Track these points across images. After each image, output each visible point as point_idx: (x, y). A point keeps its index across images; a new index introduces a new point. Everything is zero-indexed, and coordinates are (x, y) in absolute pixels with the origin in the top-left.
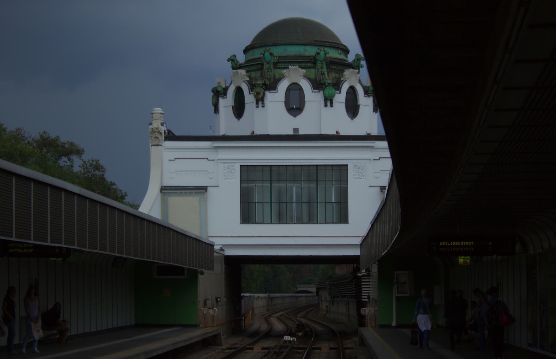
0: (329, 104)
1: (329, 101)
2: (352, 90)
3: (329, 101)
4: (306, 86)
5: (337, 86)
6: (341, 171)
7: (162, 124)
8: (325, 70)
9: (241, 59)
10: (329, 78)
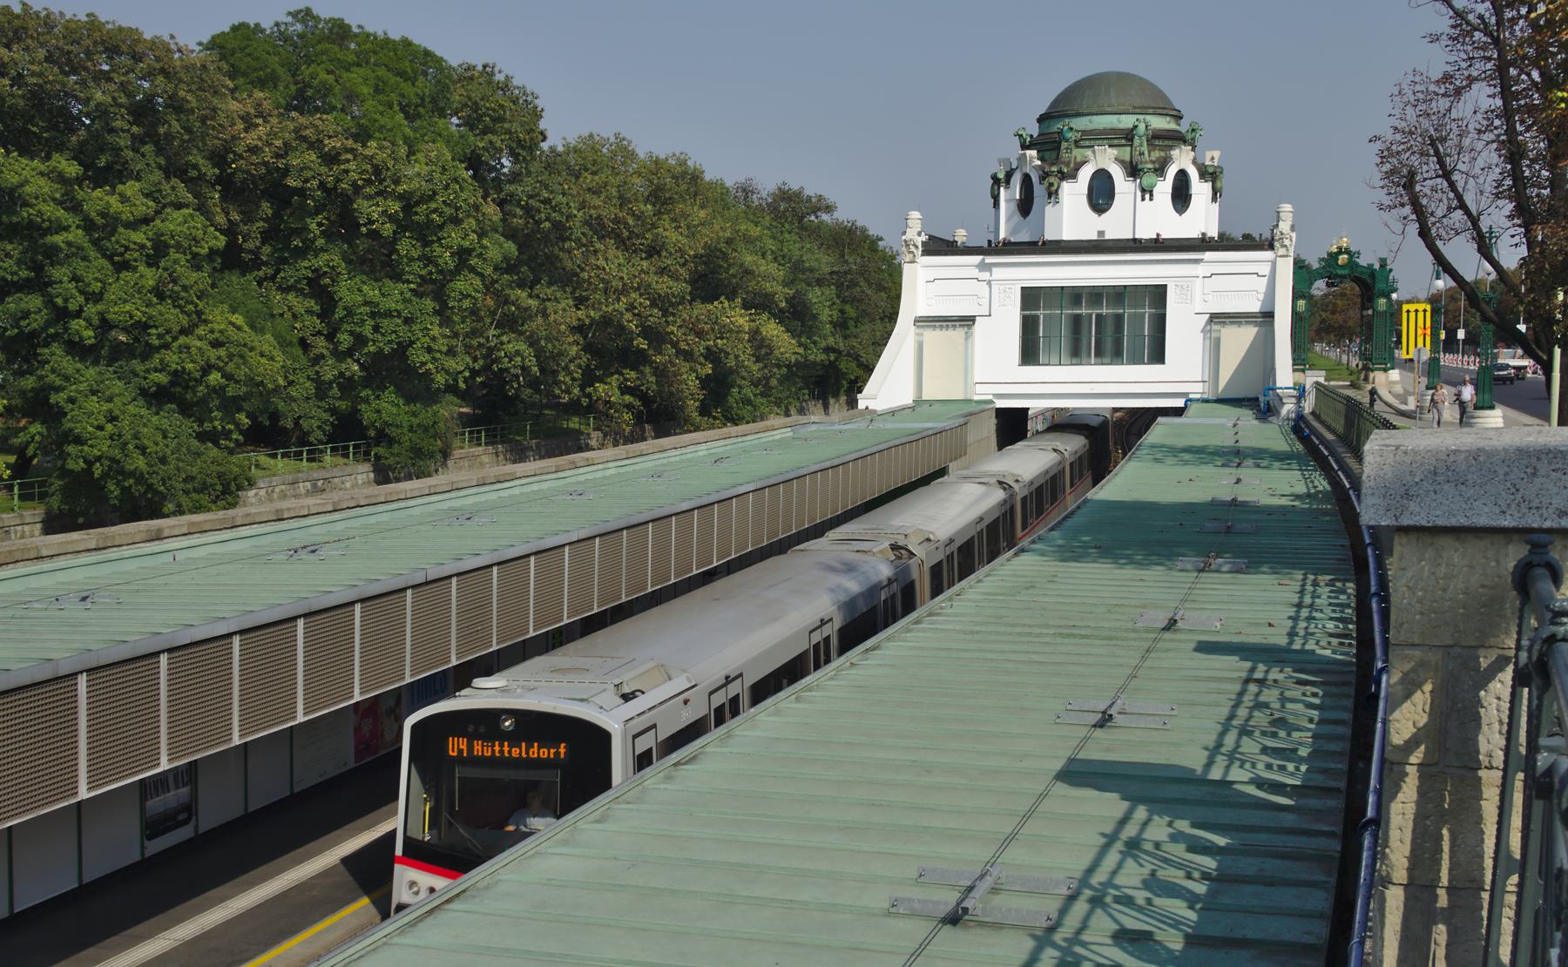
2: (1182, 177)
3: (1147, 192)
4: (1117, 173)
5: (1160, 171)
6: (1158, 294)
7: (919, 234)
8: (1145, 149)
9: (1034, 130)
10: (1149, 157)
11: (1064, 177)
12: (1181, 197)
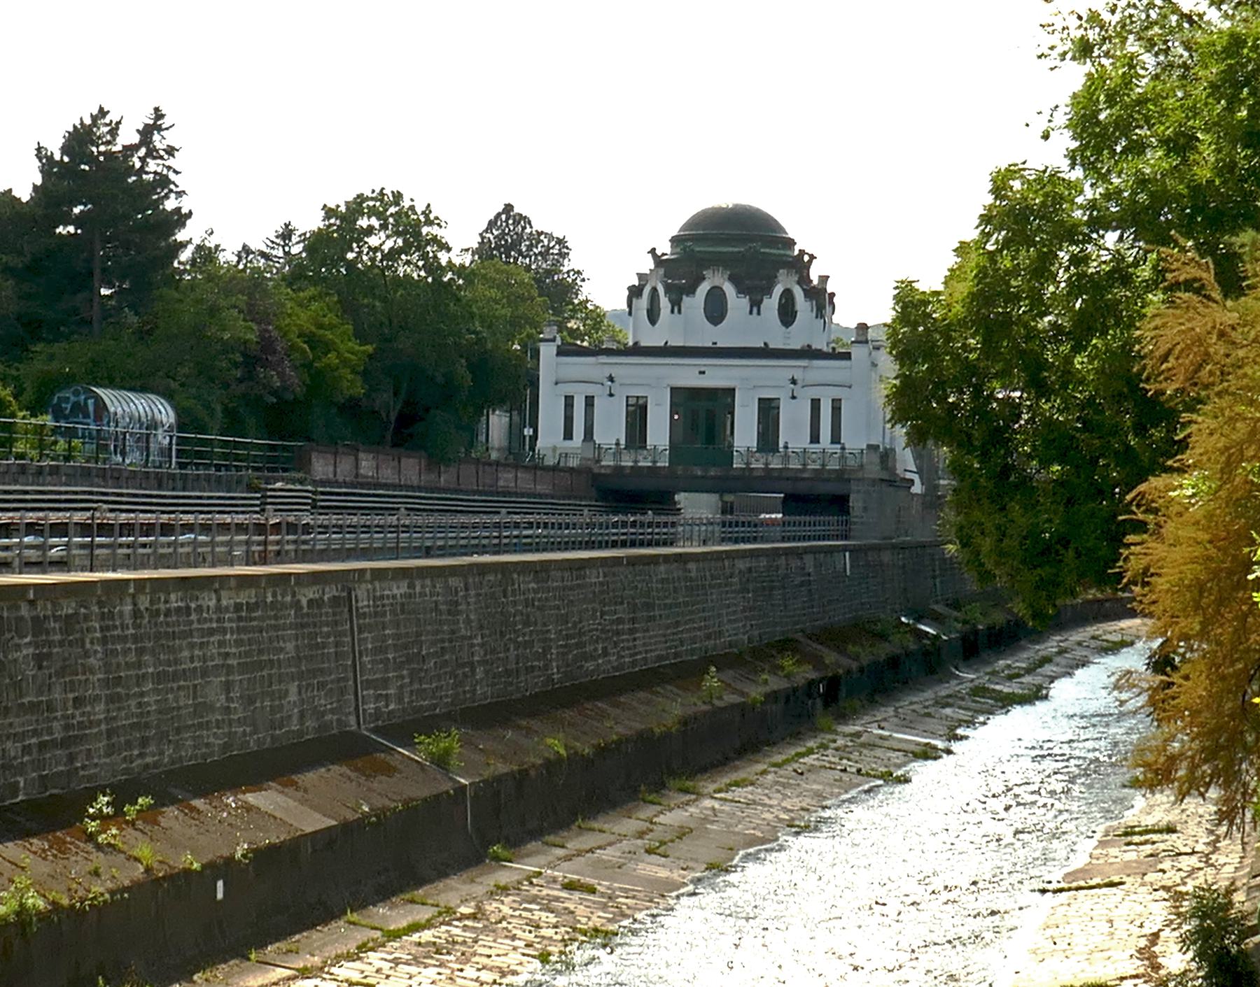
0: (755, 310)
1: (756, 304)
2: (788, 294)
3: (756, 304)
4: (729, 289)
12: (787, 314)
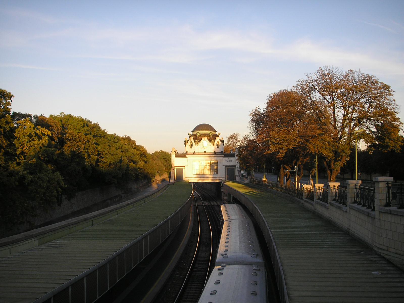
5: (214, 141)
9: (191, 134)
11: (198, 142)
